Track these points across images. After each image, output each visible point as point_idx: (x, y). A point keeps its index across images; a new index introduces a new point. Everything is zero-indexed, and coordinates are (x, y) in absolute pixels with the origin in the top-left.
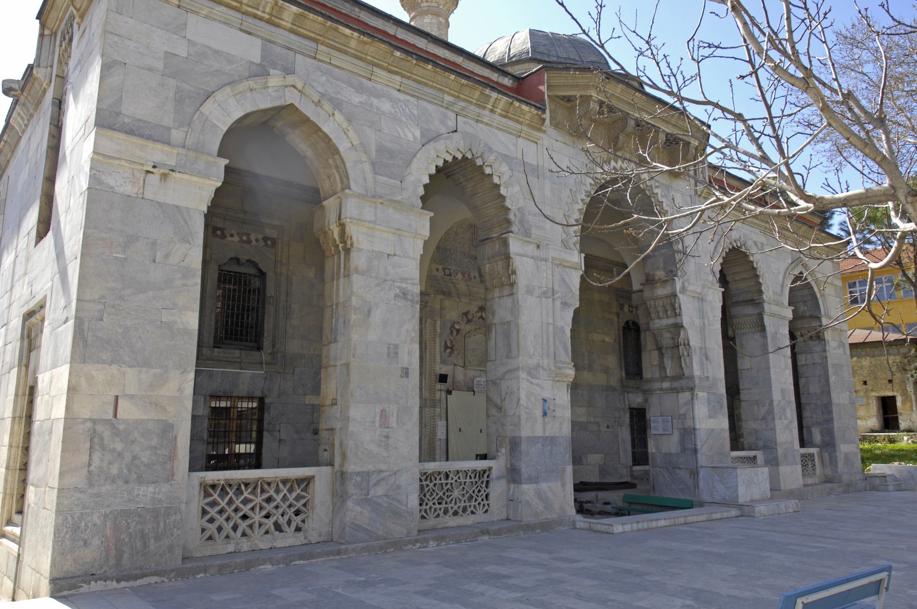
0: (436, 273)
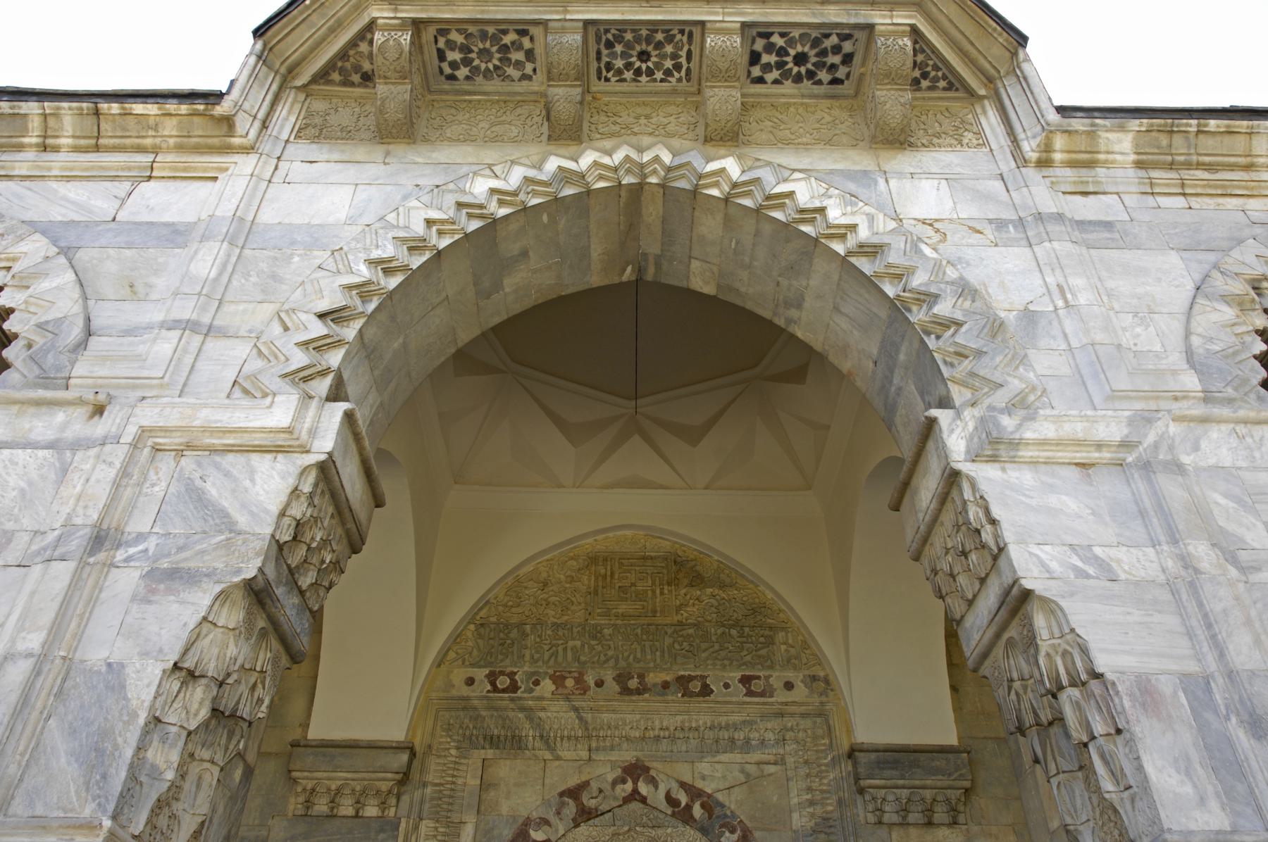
0: (466, 691)
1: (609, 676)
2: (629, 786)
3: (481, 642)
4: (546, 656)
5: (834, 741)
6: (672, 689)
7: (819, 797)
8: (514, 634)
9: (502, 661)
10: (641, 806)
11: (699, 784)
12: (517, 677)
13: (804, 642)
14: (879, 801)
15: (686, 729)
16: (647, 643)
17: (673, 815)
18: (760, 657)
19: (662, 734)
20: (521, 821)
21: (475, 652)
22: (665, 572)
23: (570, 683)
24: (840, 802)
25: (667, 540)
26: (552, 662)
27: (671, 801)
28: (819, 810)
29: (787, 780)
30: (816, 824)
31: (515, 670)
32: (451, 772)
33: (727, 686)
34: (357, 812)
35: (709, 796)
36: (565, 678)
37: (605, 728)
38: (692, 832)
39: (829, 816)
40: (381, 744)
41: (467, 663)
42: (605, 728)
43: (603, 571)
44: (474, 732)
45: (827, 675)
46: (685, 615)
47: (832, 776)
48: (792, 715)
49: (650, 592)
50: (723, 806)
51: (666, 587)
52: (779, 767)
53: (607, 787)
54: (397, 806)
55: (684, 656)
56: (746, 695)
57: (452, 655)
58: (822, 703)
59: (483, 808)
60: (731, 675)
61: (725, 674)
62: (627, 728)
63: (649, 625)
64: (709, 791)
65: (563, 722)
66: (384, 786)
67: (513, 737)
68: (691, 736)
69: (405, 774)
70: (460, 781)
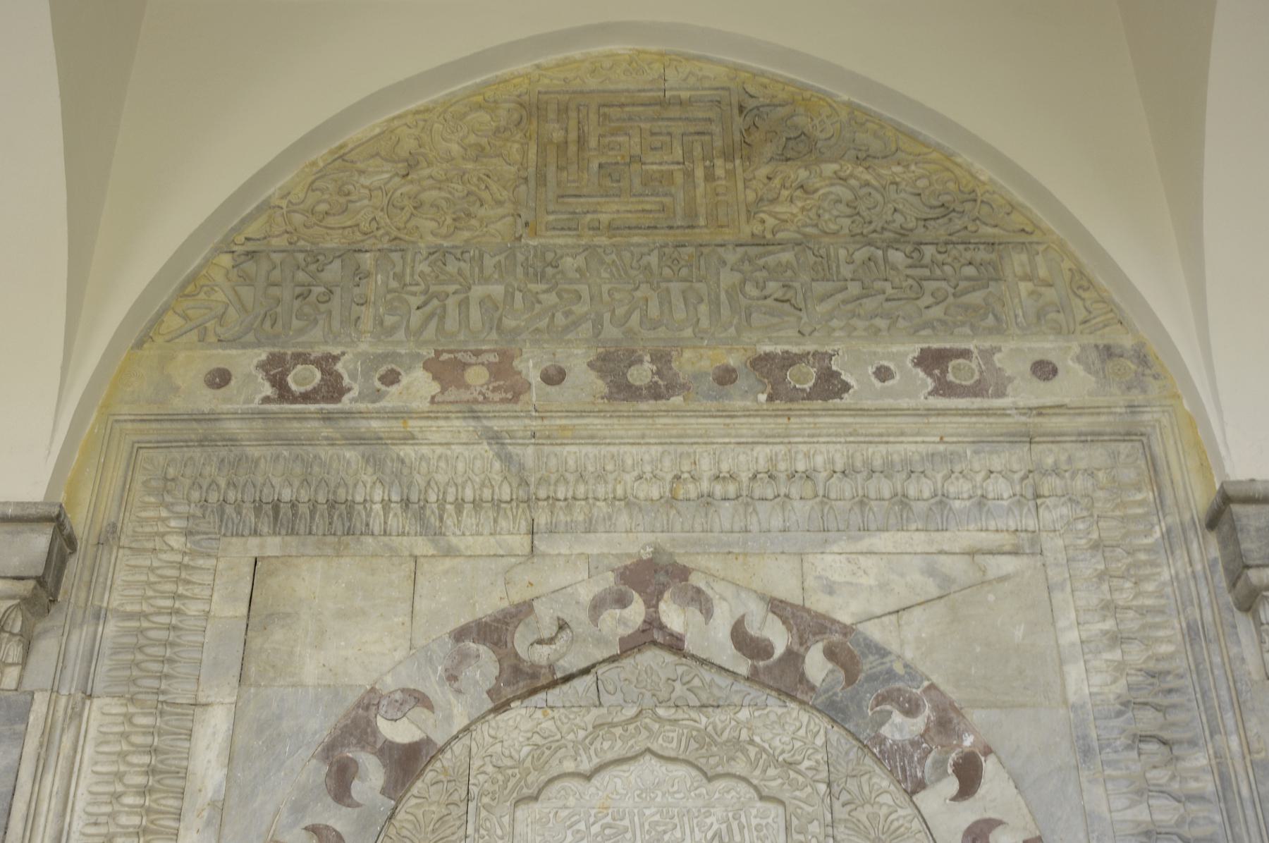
0: (207, 400)
1: (578, 360)
2: (636, 612)
3: (246, 292)
4: (416, 318)
5: (1168, 492)
6: (742, 383)
7: (1135, 626)
8: (333, 271)
9: (301, 331)
10: (669, 658)
11: (820, 603)
13: (1078, 272)
15: (783, 476)
16: (676, 287)
18: (966, 308)
19: (718, 489)
20: (352, 698)
22: (716, 128)
23: (477, 376)
24: (1193, 633)
27: (743, 640)
28: (1136, 655)
29: (1049, 589)
30: (1130, 687)
31: (336, 351)
32: (169, 587)
33: (883, 374)
35: (847, 630)
36: (465, 366)
38: (805, 717)
39: (1163, 666)
41: (212, 339)
43: (558, 136)
44: (231, 496)
45: (1142, 345)
46: (771, 222)
47: (1166, 575)
49: (679, 178)
50: (882, 652)
53: (578, 617)
54: (24, 663)
56: (934, 392)
57: (173, 322)
58: (1132, 408)
59: (252, 670)
61: (879, 349)
62: (629, 478)
64: (845, 618)
67: (332, 504)
68: (794, 492)
69: (40, 581)
70: (193, 608)
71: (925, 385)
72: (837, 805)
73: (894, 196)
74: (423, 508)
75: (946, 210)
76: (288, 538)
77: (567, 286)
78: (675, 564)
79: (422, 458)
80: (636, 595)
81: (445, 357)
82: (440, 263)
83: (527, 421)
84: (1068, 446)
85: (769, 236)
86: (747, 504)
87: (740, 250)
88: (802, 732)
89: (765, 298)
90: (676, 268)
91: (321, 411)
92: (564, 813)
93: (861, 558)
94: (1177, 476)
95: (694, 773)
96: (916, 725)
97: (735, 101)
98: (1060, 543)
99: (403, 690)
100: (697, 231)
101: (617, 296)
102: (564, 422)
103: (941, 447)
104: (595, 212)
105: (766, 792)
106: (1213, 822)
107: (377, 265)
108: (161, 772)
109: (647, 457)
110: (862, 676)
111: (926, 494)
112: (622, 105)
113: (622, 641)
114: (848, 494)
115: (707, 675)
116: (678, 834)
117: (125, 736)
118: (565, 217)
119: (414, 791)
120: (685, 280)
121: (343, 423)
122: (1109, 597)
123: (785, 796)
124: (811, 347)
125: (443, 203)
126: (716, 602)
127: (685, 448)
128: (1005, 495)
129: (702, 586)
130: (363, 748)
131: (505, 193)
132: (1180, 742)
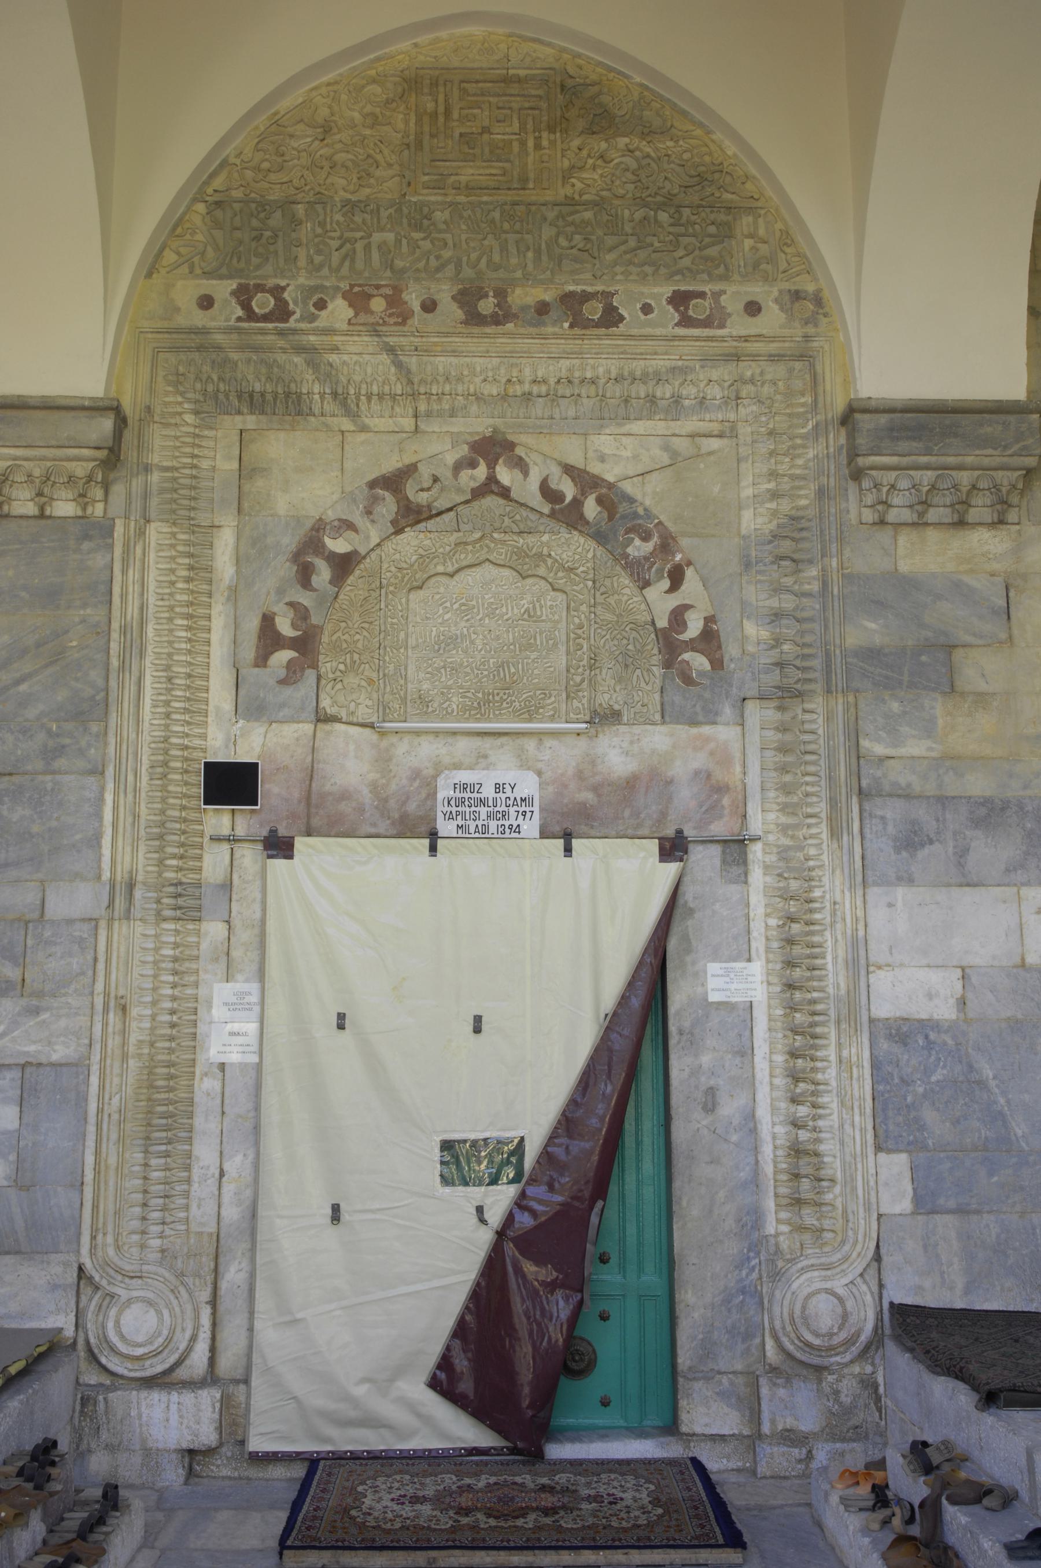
0: (200, 318)
1: (444, 293)
2: (481, 472)
3: (218, 234)
4: (336, 258)
5: (821, 399)
6: (554, 314)
7: (787, 487)
8: (276, 220)
9: (258, 267)
10: (502, 501)
11: (595, 468)
12: (286, 295)
13: (786, 233)
14: (885, 489)
15: (576, 381)
16: (512, 237)
17: (553, 515)
18: (707, 259)
20: (309, 524)
21: (210, 253)
22: (544, 105)
23: (378, 304)
24: (821, 493)
25: (549, 45)
26: (345, 270)
28: (785, 506)
29: (739, 461)
30: (779, 526)
31: (283, 283)
32: (188, 450)
33: (647, 309)
34: (42, 509)
35: (611, 486)
36: (370, 297)
37: (441, 379)
38: (582, 540)
39: (800, 513)
40: (72, 403)
41: (198, 271)
42: (441, 379)
43: (430, 106)
44: (222, 386)
45: (819, 291)
46: (579, 185)
47: (811, 454)
48: (754, 357)
50: (631, 500)
51: (545, 134)
52: (725, 441)
53: (446, 474)
54: (106, 500)
55: (575, 260)
57: (170, 257)
58: (807, 337)
59: (246, 505)
60: (656, 290)
61: (645, 290)
62: (478, 380)
63: (515, 204)
64: (610, 478)
65: (369, 370)
66: (80, 470)
67: (288, 395)
68: (584, 393)
69: (111, 450)
70: (205, 464)
71: (673, 318)
72: (598, 594)
73: (666, 166)
74: (346, 398)
75: (701, 179)
76: (260, 417)
77: (437, 235)
78: (506, 440)
79: (344, 363)
80: (481, 461)
81: (356, 289)
82: (350, 214)
83: (412, 339)
84: (762, 363)
85: (577, 197)
86: (553, 400)
87: (557, 208)
88: (579, 550)
89: (572, 248)
90: (512, 223)
91: (276, 328)
92: (437, 597)
93: (623, 438)
94: (828, 387)
95: (515, 574)
96: (649, 547)
97: (558, 80)
98: (749, 429)
99: (339, 520)
100: (527, 192)
101: (472, 244)
102: (436, 340)
103: (680, 363)
104: (457, 174)
105: (556, 586)
106: (814, 609)
107: (307, 215)
108: (197, 569)
109: (490, 366)
110: (618, 516)
111: (668, 395)
112: (477, 82)
113: (473, 490)
114: (618, 394)
115: (524, 513)
116: (504, 610)
117: (173, 546)
118: (435, 177)
119: (349, 582)
120: (518, 232)
121: (291, 337)
122: (774, 467)
123: (568, 589)
124: (600, 288)
125: (350, 164)
126: (531, 465)
127: (514, 360)
128: (718, 397)
129: (523, 455)
130: (317, 556)
131: (393, 157)
132: (802, 561)
